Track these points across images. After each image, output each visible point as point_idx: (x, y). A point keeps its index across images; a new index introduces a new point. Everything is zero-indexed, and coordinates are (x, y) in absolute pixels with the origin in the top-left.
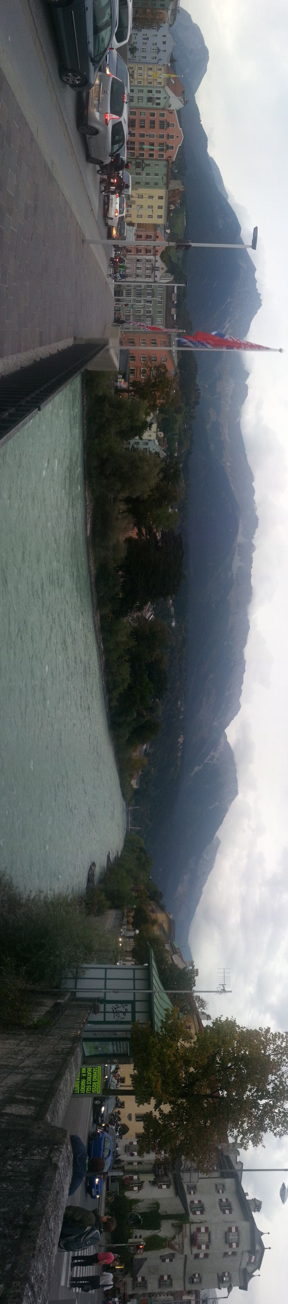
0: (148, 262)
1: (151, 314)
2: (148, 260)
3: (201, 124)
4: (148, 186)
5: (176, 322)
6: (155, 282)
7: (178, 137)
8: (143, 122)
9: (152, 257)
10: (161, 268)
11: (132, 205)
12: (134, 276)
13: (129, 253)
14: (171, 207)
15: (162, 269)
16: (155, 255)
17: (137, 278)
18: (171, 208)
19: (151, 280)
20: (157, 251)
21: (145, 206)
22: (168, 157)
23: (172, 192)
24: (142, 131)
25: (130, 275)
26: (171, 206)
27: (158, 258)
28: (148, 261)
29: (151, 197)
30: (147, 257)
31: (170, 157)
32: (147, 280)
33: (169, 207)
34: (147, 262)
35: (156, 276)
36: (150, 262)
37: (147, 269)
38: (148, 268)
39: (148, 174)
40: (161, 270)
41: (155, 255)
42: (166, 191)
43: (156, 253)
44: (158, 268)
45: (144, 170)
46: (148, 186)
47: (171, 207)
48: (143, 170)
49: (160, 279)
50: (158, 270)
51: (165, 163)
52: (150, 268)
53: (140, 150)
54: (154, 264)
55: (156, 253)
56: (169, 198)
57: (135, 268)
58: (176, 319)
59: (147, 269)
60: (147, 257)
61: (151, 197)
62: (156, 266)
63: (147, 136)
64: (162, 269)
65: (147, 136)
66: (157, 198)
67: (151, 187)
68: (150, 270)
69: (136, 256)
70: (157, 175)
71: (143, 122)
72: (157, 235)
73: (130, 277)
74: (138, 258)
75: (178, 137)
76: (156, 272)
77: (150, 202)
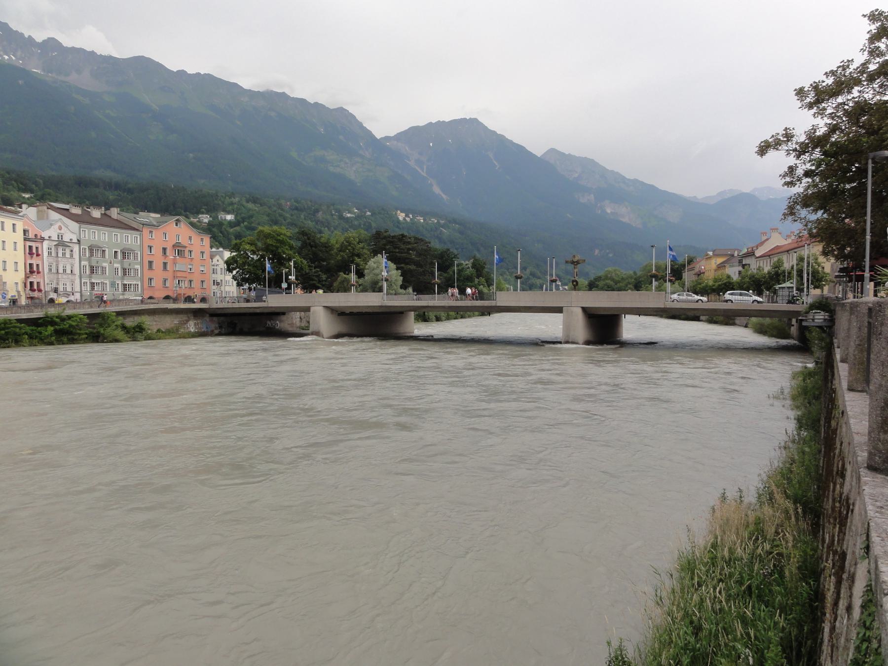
1: (119, 251)
9: (46, 244)
10: (59, 232)
15: (60, 228)
19: (76, 248)
20: (36, 235)
28: (50, 254)
30: (46, 254)
35: (71, 240)
37: (64, 254)
40: (62, 231)
43: (39, 237)
44: (58, 236)
54: (56, 243)
55: (39, 237)
59: (64, 254)
60: (46, 254)
64: (60, 228)
76: (64, 240)
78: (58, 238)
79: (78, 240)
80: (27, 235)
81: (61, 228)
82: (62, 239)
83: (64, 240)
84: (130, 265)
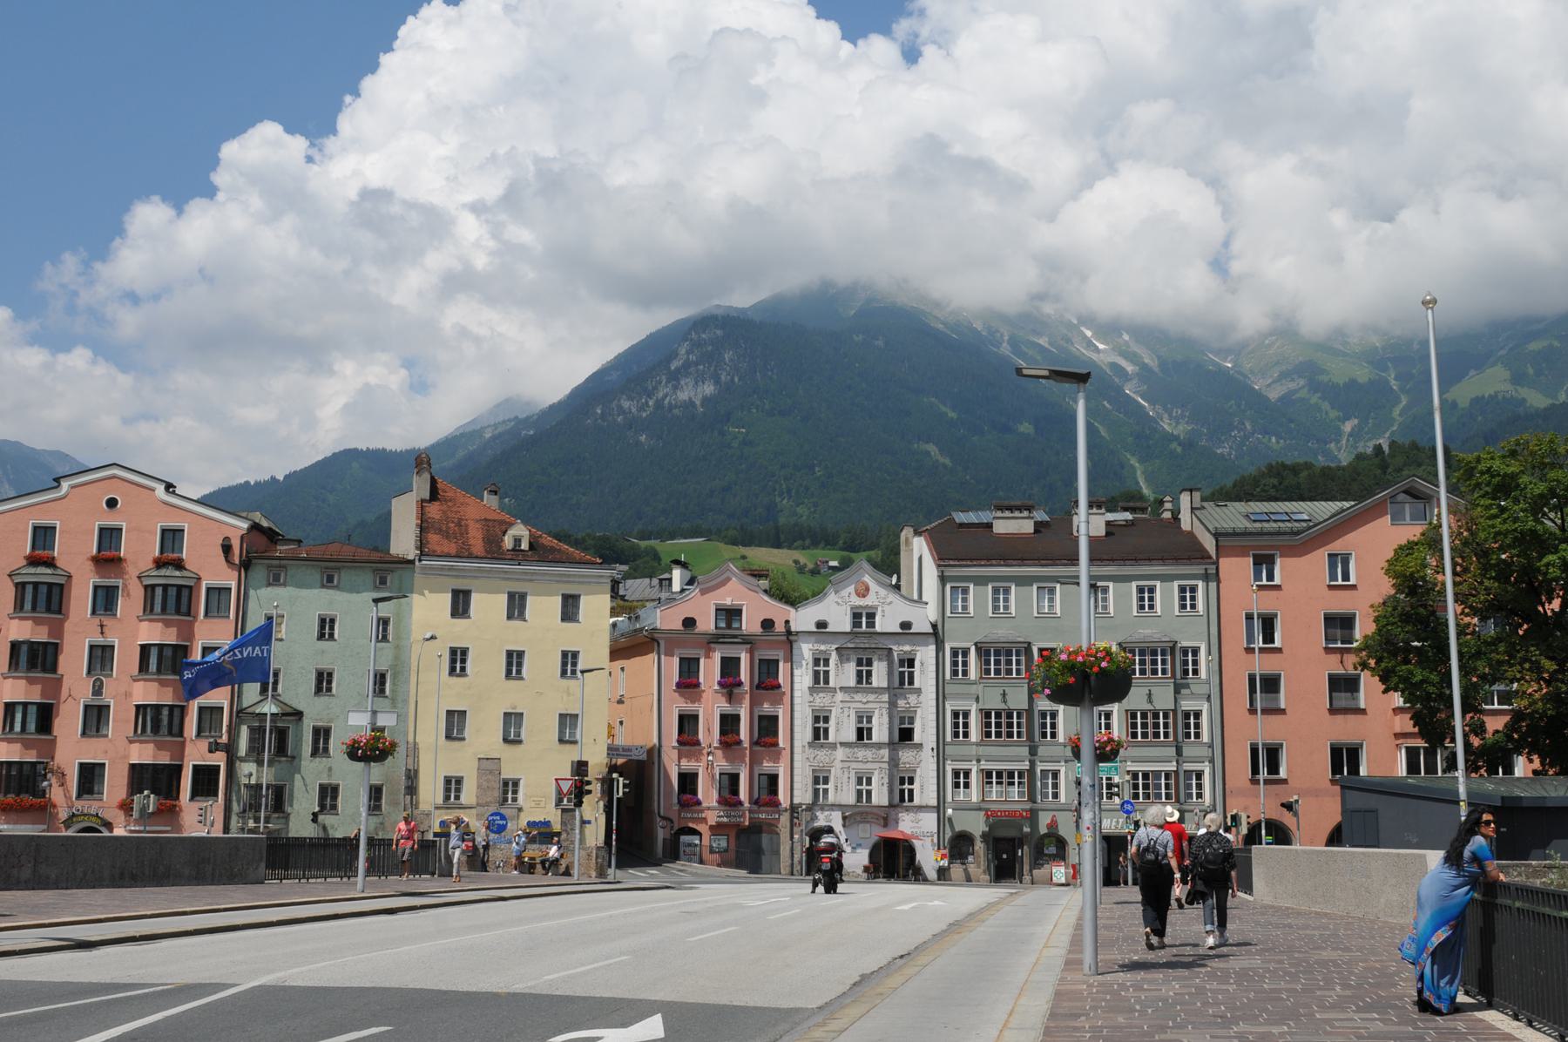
0: (827, 673)
2: (816, 674)
3: (286, 477)
4: (395, 677)
5: (1143, 510)
6: (936, 635)
7: (112, 503)
8: (18, 717)
9: (806, 650)
11: (507, 774)
12: (906, 756)
13: (783, 796)
14: (517, 541)
16: (790, 638)
17: (917, 738)
18: (525, 546)
19: (926, 655)
20: (768, 624)
21: (512, 696)
22: (227, 560)
23: (433, 538)
24: (68, 722)
25: (902, 781)
26: (508, 542)
27: (803, 618)
28: (820, 680)
29: (458, 659)
31: (227, 548)
32: (925, 676)
33: (516, 554)
34: (827, 681)
35: (906, 625)
36: (827, 662)
37: (863, 677)
38: (859, 674)
39: (323, 681)
41: (790, 638)
42: (427, 571)
44: (856, 616)
45: (300, 708)
46: (395, 677)
47: (517, 541)
48: (298, 715)
49: (920, 601)
50: (871, 616)
51: (259, 572)
52: (860, 663)
53: (181, 734)
55: (780, 627)
56: (465, 554)
57: (861, 753)
58: (1125, 509)
59: (863, 677)
61: (458, 659)
62: (848, 628)
63: (98, 691)
64: (863, 592)
65: (98, 691)
66: (461, 623)
67: (400, 666)
68: (869, 663)
69: (797, 750)
70: (326, 628)
71: (18, 717)
72: (678, 625)
73: (911, 781)
74: (809, 735)
75: (112, 503)
76: (878, 628)
77: (486, 665)
78: (856, 624)
79: (934, 626)
80: (735, 625)
81: (867, 589)
82: (871, 624)
83: (878, 628)
84: (1150, 701)
